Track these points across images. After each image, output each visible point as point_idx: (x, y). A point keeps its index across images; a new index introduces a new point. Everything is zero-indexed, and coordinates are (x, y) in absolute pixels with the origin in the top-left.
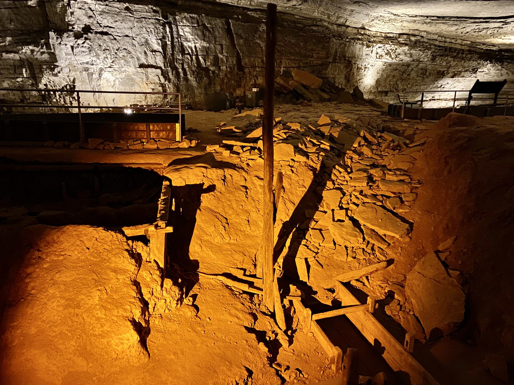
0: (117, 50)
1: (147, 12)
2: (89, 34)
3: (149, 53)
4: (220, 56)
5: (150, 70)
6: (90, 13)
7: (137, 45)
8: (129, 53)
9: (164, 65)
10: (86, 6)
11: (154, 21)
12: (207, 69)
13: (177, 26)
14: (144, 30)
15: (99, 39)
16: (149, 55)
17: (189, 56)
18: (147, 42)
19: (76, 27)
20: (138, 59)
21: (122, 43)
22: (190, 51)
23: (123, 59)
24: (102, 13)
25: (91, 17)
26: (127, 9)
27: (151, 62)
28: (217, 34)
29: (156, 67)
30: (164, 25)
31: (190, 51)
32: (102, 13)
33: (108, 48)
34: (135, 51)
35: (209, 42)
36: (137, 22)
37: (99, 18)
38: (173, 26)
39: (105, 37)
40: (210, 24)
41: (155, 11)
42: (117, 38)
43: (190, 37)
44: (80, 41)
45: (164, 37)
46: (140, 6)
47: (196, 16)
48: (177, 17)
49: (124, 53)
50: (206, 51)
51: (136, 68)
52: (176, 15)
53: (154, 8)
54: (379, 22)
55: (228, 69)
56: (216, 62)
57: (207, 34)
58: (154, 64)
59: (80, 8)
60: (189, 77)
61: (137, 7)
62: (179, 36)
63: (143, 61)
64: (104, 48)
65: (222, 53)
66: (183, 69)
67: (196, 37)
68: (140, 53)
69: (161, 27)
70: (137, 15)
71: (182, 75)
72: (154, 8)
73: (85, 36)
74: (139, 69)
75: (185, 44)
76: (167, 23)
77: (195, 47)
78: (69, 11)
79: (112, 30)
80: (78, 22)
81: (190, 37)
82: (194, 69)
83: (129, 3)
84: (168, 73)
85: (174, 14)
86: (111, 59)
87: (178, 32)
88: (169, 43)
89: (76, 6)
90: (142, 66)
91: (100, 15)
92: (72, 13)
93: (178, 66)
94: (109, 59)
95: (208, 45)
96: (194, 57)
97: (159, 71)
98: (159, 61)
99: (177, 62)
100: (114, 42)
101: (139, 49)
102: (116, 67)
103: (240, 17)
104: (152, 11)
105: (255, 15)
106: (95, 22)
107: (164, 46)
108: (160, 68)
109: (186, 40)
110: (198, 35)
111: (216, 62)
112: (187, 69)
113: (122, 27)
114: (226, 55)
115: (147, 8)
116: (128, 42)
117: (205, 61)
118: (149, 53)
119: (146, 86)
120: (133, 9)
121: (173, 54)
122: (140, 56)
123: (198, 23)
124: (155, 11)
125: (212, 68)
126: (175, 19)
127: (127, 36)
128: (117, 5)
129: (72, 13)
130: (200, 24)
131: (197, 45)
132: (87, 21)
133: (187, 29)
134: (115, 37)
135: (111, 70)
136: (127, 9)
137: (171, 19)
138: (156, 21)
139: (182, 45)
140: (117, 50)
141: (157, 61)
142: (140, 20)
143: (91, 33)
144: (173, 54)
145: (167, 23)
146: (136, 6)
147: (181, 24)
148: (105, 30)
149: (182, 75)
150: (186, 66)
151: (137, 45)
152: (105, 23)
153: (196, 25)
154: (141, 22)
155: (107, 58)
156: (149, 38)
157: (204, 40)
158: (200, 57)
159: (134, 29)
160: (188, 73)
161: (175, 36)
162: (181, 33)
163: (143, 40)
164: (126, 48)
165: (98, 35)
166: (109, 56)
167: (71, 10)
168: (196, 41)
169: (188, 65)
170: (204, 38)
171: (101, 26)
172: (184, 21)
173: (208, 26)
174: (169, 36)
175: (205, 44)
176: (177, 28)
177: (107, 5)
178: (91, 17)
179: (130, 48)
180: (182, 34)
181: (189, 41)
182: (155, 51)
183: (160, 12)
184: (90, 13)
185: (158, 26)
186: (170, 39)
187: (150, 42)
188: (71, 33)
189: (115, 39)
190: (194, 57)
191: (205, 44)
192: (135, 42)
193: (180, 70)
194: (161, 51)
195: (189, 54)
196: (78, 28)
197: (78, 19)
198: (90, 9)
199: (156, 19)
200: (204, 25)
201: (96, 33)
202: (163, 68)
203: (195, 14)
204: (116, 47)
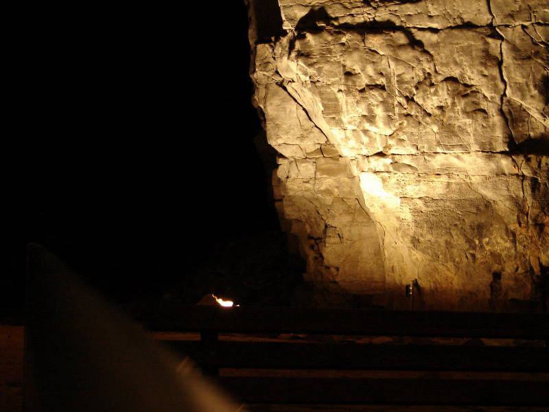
20: (512, 117)
33: (381, 81)
39: (375, 41)
42: (426, 38)
51: (488, 152)
64: (364, 81)
100: (407, 55)
101: (515, 73)
116: (466, 51)
127: (468, 26)
134: (419, 36)
164: (456, 73)
166: (379, 112)
179: (473, 77)
189: (415, 43)
201: (347, 28)
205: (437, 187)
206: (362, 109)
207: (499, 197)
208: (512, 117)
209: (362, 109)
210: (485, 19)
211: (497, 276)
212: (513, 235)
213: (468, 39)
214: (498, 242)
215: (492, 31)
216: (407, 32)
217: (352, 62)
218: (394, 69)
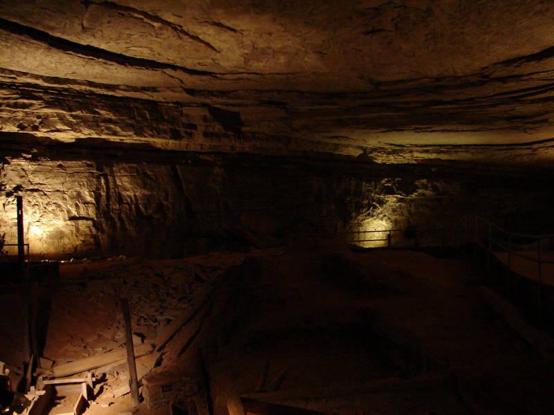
0: (47, 205)
1: (80, 167)
2: (20, 192)
3: (81, 205)
4: (164, 203)
5: (80, 222)
6: (23, 173)
7: (68, 198)
8: (59, 206)
9: (97, 217)
10: (19, 168)
11: (87, 175)
12: (150, 218)
13: (114, 177)
14: (77, 183)
15: (29, 196)
16: (81, 207)
17: (127, 206)
18: (79, 196)
19: (7, 186)
20: (69, 212)
21: (52, 198)
22: (129, 200)
23: (52, 213)
24: (34, 172)
25: (23, 176)
26: (60, 166)
27: (83, 213)
28: (161, 180)
29: (87, 219)
30: (98, 178)
31: (129, 200)
32: (34, 172)
34: (66, 204)
35: (152, 190)
36: (69, 177)
37: (31, 177)
38: (109, 177)
39: (35, 194)
40: (152, 171)
41: (88, 165)
43: (128, 185)
44: (10, 199)
45: (98, 189)
46: (74, 162)
47: (135, 165)
48: (114, 169)
49: (54, 207)
50: (148, 199)
51: (65, 220)
52: (112, 166)
53: (89, 163)
54: (379, 154)
55: (176, 216)
56: (160, 208)
57: (149, 182)
58: (86, 216)
59: (12, 170)
60: (127, 226)
61: (69, 163)
62: (116, 186)
63: (74, 213)
64: (33, 203)
65: (167, 200)
66: (120, 218)
67: (136, 186)
68: (71, 206)
69: (95, 180)
70: (69, 171)
71: (118, 225)
72: (89, 163)
73: (15, 194)
74: (69, 222)
75: (124, 193)
76: (102, 175)
77: (135, 196)
78: (3, 173)
79: (43, 186)
80: (10, 182)
81: (128, 185)
82: (132, 218)
83: (63, 159)
84: (101, 225)
85: (111, 166)
86: (40, 213)
87: (115, 182)
88: (103, 194)
89: (10, 168)
90: (72, 218)
91: (32, 174)
92: (5, 175)
93: (114, 216)
94: (38, 213)
95: (150, 193)
96: (133, 206)
97: (90, 223)
98: (92, 212)
99: (113, 212)
100: (44, 197)
102: (44, 220)
103: (190, 161)
104: (85, 165)
105: (208, 158)
106: (26, 181)
107: (98, 197)
108: (92, 219)
109: (125, 189)
110: (137, 184)
111: (160, 208)
112: (125, 219)
113: (53, 183)
114: (172, 201)
115: (80, 163)
116: (59, 197)
117: (146, 209)
118: (81, 205)
119: (76, 238)
120: (66, 165)
121: (108, 205)
122: (70, 208)
123: (137, 172)
124: (88, 165)
125: (156, 216)
126: (112, 171)
127: (58, 191)
128: (50, 163)
129: (5, 175)
130: (140, 172)
131: (137, 194)
132: (18, 181)
133: (125, 179)
135: (38, 224)
136: (60, 166)
137: (107, 171)
138: (90, 174)
139: (120, 195)
140: (47, 205)
141: (90, 212)
142: (72, 175)
143: (21, 191)
144: (108, 205)
145: (102, 175)
146: (69, 162)
147: (119, 174)
148: (36, 187)
149: (118, 225)
150: (123, 216)
151: (68, 198)
152: (37, 180)
153: (135, 174)
154: (74, 176)
155: (35, 212)
156: (81, 191)
157: (144, 188)
158: (140, 206)
159: (65, 184)
160: (126, 223)
161: (111, 185)
162: (119, 183)
163: (75, 193)
165: (28, 192)
166: (38, 211)
167: (4, 173)
168: (135, 190)
169: (127, 215)
170: (144, 186)
171: (32, 184)
172: (122, 171)
173: (151, 173)
174: (105, 187)
175: (146, 192)
176: (114, 179)
177: (40, 165)
178: (23, 176)
179: (60, 202)
180: (120, 184)
181: (128, 191)
182: (88, 203)
183: (95, 166)
184: (23, 173)
185: (91, 179)
186: (105, 190)
187: (82, 194)
188: (3, 192)
189: (45, 195)
190: (133, 206)
191: (146, 192)
192: (66, 196)
193: (117, 220)
194: (94, 202)
195: (127, 203)
196: (9, 188)
197: (11, 180)
198: (23, 169)
199: (90, 172)
200: (145, 174)
201: (28, 190)
202: (95, 219)
203: (136, 163)
204: (46, 202)
205: (51, 229)
206: (33, 210)
207: (67, 231)
208: (69, 212)
209: (33, 210)
210: (62, 189)
211: (64, 248)
212: (69, 239)
213: (58, 194)
214: (66, 241)
215: (64, 192)
216: (43, 191)
217: (30, 199)
218: (40, 200)
